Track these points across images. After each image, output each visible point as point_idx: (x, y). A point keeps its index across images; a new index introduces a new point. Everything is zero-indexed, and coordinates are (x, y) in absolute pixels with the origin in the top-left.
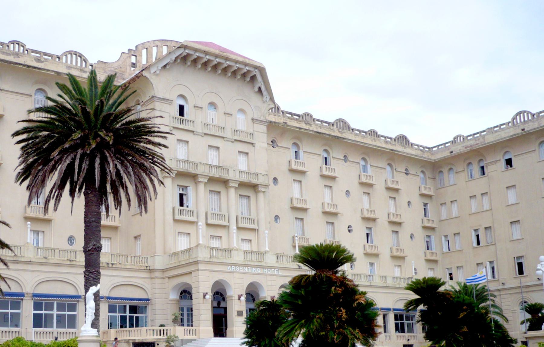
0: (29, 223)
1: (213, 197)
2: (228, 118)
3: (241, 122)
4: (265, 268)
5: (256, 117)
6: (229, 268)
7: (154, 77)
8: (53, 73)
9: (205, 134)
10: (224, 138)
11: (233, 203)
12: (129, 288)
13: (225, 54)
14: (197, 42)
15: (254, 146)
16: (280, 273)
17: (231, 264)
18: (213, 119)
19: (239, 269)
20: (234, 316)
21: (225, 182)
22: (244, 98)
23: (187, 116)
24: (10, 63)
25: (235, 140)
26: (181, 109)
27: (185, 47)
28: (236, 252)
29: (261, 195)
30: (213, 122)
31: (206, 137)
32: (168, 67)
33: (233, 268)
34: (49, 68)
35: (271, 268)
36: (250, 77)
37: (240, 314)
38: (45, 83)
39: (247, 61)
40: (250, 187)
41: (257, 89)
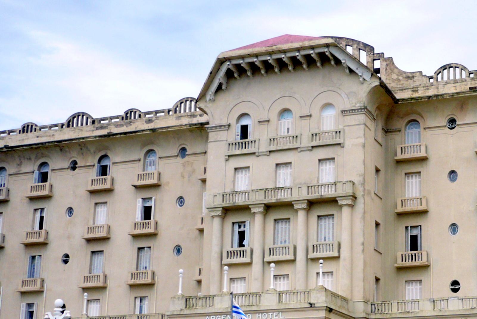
0: (86, 294)
1: (284, 226)
2: (306, 121)
3: (329, 121)
5: (348, 107)
7: (210, 104)
8: (148, 132)
9: (270, 152)
10: (297, 149)
11: (299, 230)
13: (274, 47)
14: (253, 46)
15: (343, 147)
18: (288, 129)
21: (288, 205)
22: (330, 89)
23: (250, 138)
24: (125, 133)
25: (313, 147)
26: (244, 131)
27: (229, 59)
28: (220, 298)
29: (346, 211)
30: (288, 132)
31: (273, 155)
32: (224, 87)
34: (143, 129)
36: (321, 59)
38: (152, 143)
39: (307, 44)
40: (321, 205)
41: (347, 71)
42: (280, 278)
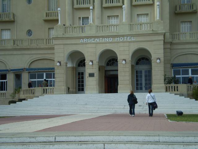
4: (117, 37)
6: (81, 41)
12: (45, 62)
16: (133, 39)
17: (83, 38)
19: (92, 40)
20: (86, 78)
33: (85, 40)
35: (123, 36)
37: (91, 75)
42: (112, 18)
